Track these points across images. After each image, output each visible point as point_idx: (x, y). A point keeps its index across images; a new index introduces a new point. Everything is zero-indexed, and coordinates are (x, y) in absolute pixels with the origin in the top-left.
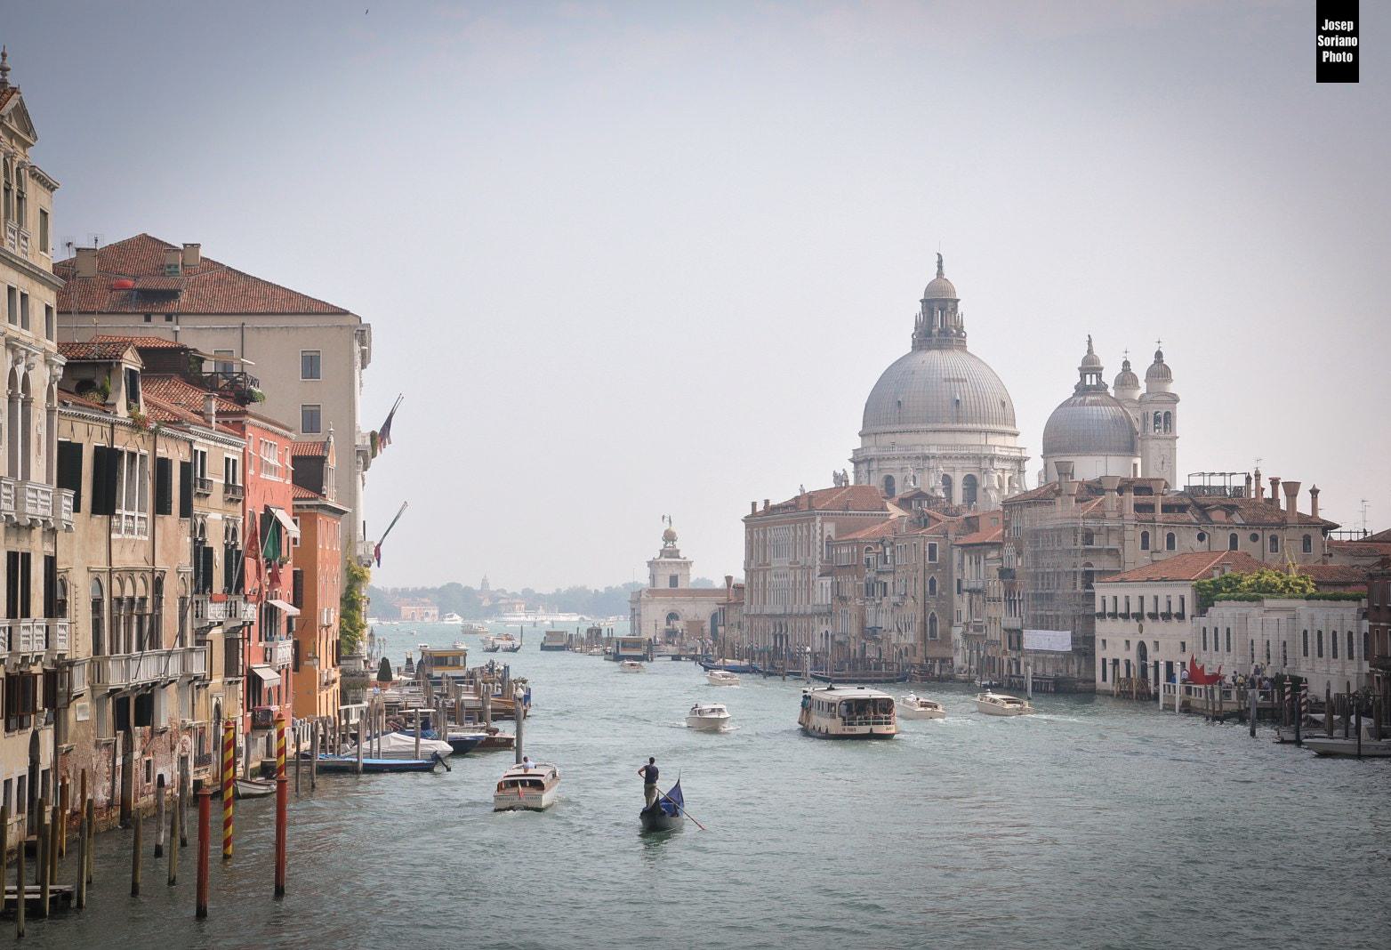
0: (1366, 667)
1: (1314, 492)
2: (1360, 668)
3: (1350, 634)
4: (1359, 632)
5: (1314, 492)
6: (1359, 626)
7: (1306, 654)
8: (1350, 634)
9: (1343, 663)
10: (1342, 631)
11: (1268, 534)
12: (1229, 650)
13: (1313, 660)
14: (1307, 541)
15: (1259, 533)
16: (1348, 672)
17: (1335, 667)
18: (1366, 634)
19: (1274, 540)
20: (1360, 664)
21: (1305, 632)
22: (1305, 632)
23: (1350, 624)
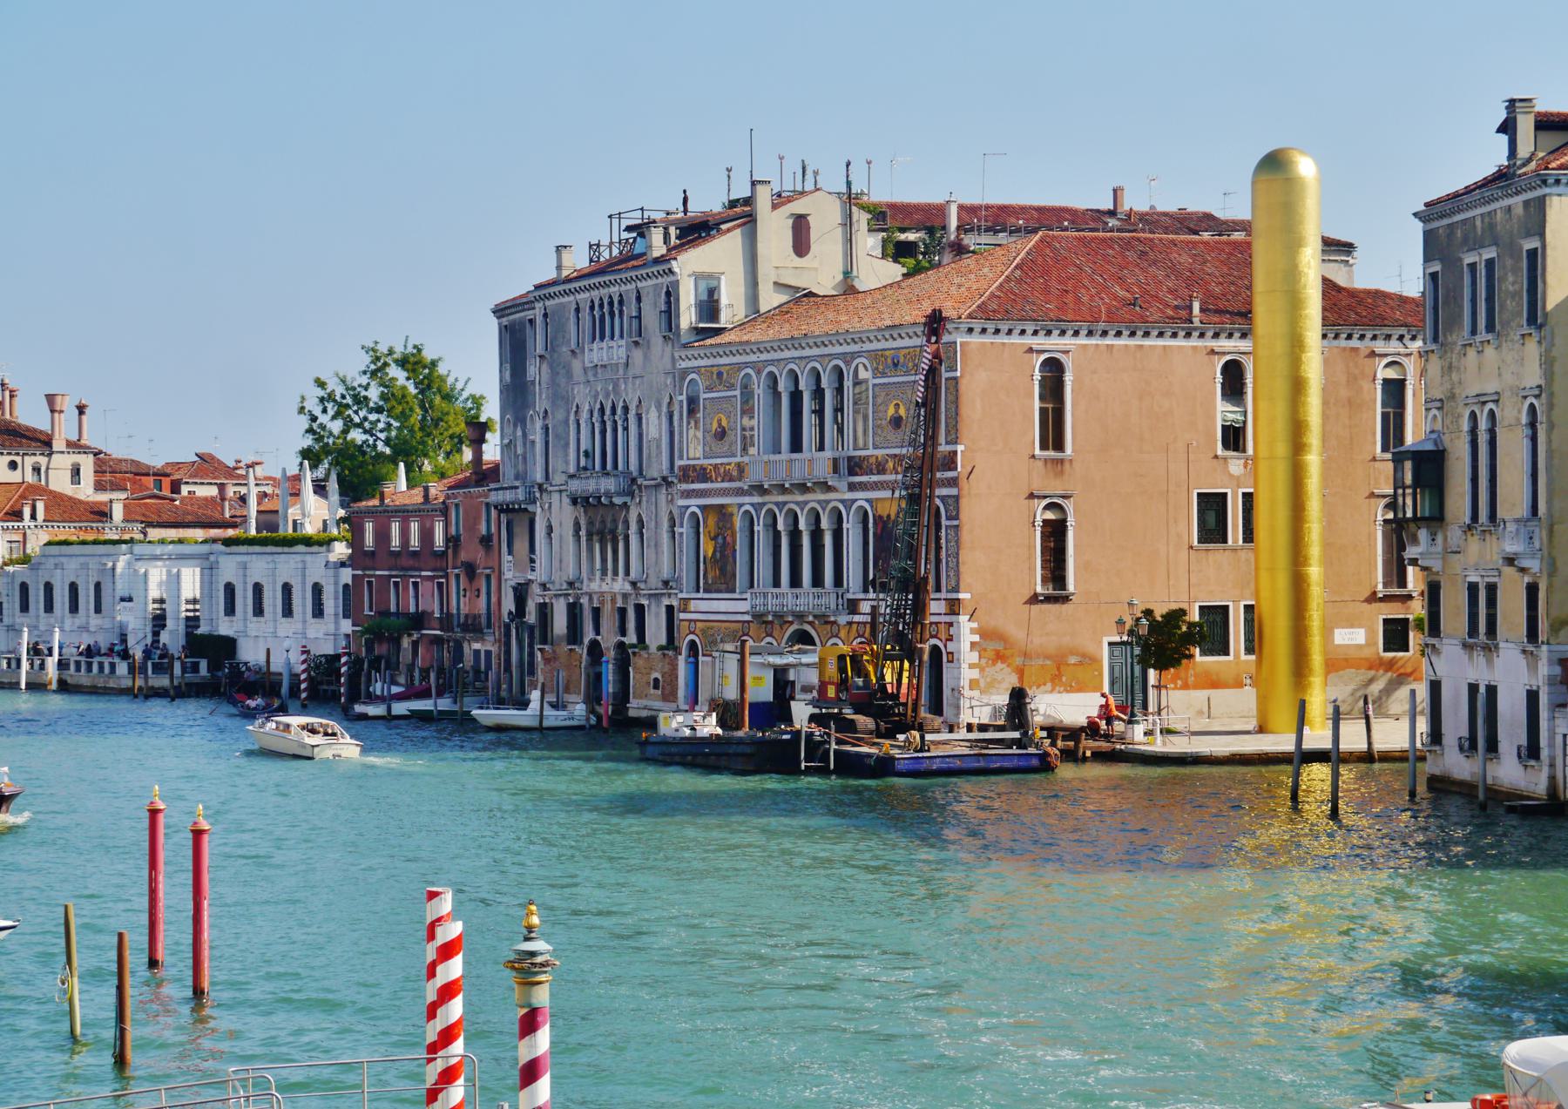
0: (347, 626)
1: (81, 409)
2: (337, 629)
3: (317, 590)
4: (336, 583)
5: (81, 409)
6: (336, 576)
7: (230, 610)
8: (317, 590)
9: (305, 622)
10: (304, 583)
11: (29, 461)
12: (98, 610)
13: (245, 619)
14: (76, 472)
15: (18, 459)
16: (311, 634)
17: (286, 627)
18: (346, 586)
19: (36, 470)
20: (337, 623)
21: (230, 590)
22: (230, 590)
23: (317, 573)
